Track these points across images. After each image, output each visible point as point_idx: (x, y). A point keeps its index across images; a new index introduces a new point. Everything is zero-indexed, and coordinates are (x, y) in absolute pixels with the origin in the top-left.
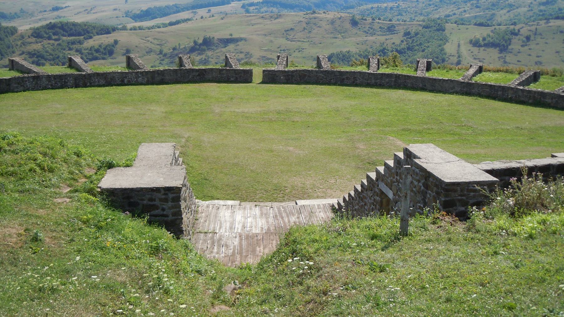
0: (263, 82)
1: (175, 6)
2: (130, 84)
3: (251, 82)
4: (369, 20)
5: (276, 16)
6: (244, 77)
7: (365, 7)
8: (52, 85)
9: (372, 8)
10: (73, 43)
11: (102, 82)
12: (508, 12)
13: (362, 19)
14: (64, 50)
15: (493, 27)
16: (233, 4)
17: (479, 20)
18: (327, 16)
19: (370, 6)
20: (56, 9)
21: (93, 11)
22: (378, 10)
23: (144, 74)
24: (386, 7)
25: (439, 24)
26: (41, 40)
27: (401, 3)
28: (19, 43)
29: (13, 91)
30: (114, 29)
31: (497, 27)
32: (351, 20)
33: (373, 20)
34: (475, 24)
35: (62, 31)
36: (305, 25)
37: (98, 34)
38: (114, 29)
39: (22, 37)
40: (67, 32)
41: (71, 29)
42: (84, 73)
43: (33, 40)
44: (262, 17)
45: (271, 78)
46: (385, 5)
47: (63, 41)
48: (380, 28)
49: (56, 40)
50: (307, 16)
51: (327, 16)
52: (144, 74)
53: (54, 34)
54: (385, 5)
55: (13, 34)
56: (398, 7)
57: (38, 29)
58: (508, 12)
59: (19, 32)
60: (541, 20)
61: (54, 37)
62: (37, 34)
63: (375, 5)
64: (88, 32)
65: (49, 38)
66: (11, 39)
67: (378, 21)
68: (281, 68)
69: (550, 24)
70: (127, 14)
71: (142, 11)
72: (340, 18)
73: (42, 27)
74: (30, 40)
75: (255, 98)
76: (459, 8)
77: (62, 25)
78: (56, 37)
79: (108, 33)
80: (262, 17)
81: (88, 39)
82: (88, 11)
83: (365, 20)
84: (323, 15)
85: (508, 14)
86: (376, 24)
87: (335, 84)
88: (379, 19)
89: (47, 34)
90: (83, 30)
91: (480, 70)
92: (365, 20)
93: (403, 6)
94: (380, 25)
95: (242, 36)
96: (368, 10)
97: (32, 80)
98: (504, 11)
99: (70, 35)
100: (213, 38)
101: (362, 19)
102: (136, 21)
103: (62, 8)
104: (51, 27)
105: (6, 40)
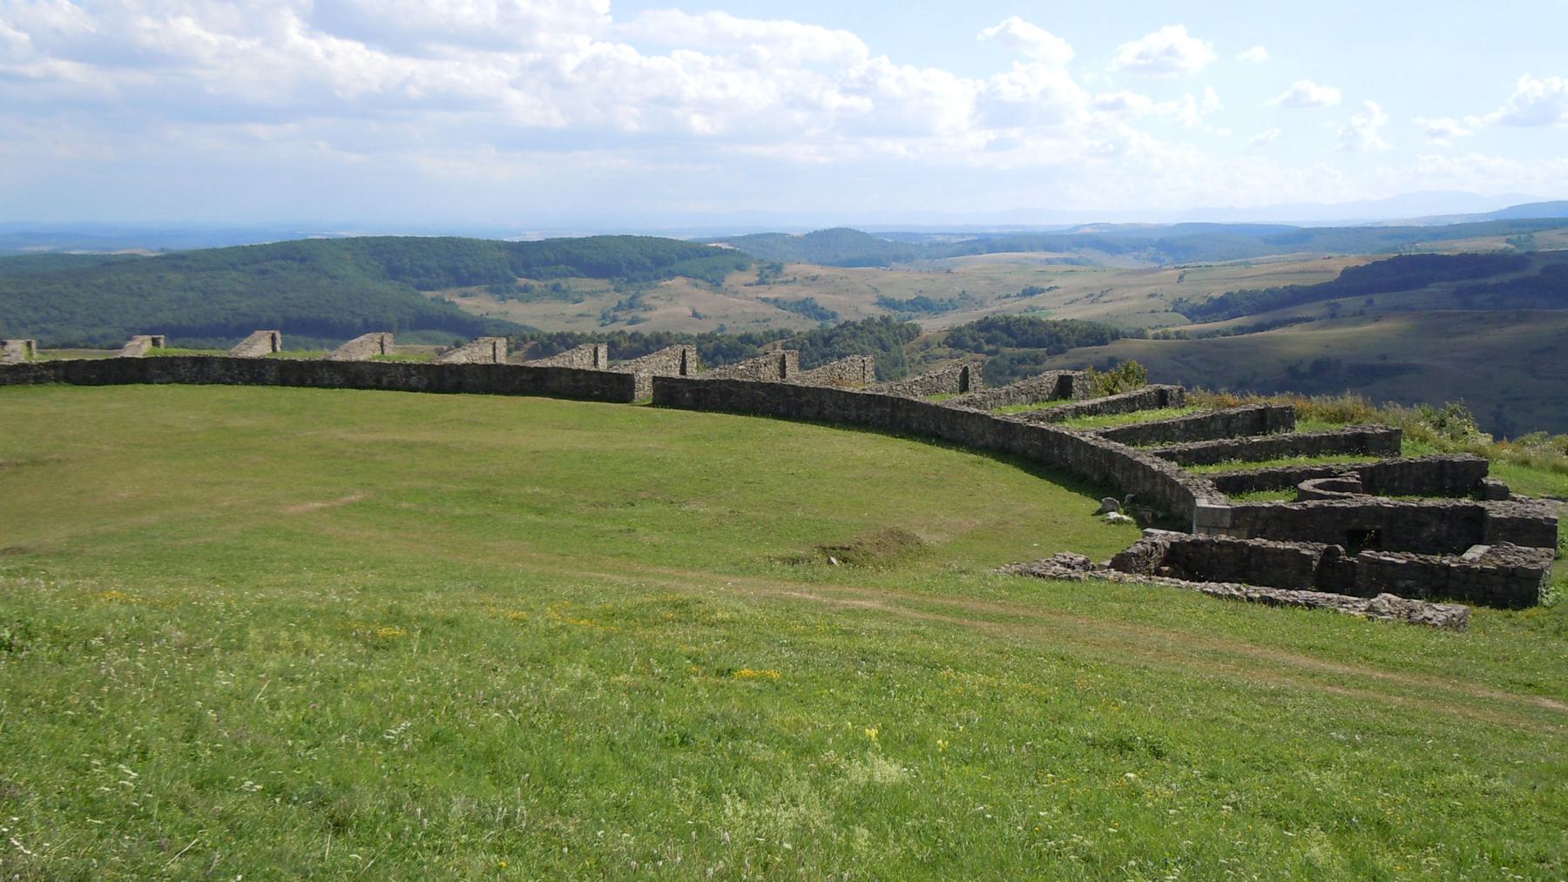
1: (1291, 289)
10: (1022, 361)
14: (1001, 373)
16: (1433, 288)
20: (1030, 292)
21: (1105, 298)
26: (959, 351)
28: (918, 357)
30: (1116, 336)
35: (1005, 336)
37: (1079, 345)
38: (1116, 336)
39: (927, 345)
40: (1015, 338)
41: (1026, 332)
43: (946, 351)
47: (1003, 356)
49: (988, 353)
53: (988, 342)
55: (910, 338)
57: (959, 330)
59: (924, 334)
61: (986, 348)
62: (955, 340)
64: (1059, 340)
65: (978, 350)
66: (905, 348)
70: (1177, 306)
71: (1211, 299)
73: (970, 326)
74: (939, 351)
77: (1008, 323)
78: (991, 347)
79: (1103, 342)
81: (1055, 353)
82: (1093, 299)
89: (974, 340)
90: (1050, 335)
95: (1416, 361)
99: (1019, 345)
100: (1338, 362)
102: (1194, 322)
103: (1043, 291)
104: (986, 326)
105: (894, 349)
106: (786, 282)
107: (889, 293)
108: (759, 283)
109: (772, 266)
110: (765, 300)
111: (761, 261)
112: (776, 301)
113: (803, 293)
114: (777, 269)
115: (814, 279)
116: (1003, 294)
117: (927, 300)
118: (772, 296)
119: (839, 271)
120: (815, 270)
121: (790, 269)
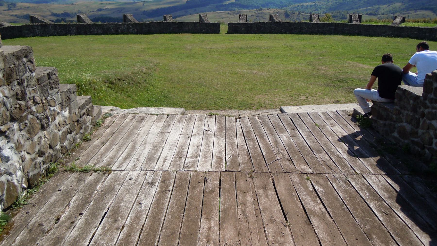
0: (228, 33)
2: (123, 33)
3: (219, 33)
4: (297, 13)
5: (237, 12)
6: (213, 28)
7: (293, 6)
8: (57, 33)
9: (298, 6)
11: (100, 31)
12: (389, 6)
13: (292, 13)
15: (379, 16)
17: (369, 12)
18: (269, 11)
19: (297, 5)
22: (302, 8)
23: (134, 25)
24: (307, 5)
25: (343, 15)
27: (317, 2)
29: (24, 36)
31: (382, 16)
32: (285, 14)
33: (299, 13)
34: (367, 14)
36: (255, 18)
42: (85, 24)
44: (228, 13)
45: (234, 29)
46: (307, 4)
48: (304, 18)
50: (257, 12)
51: (269, 11)
52: (134, 25)
54: (307, 4)
56: (315, 5)
58: (389, 6)
60: (411, 10)
63: (300, 4)
67: (302, 13)
68: (244, 22)
69: (417, 13)
72: (277, 13)
75: (222, 41)
76: (356, 5)
80: (228, 13)
83: (294, 13)
84: (266, 11)
85: (388, 8)
86: (301, 16)
87: (285, 33)
88: (303, 12)
91: (403, 20)
92: (294, 13)
93: (319, 4)
94: (304, 16)
96: (295, 7)
97: (40, 28)
98: (386, 6)
101: (292, 13)
106: (18, 9)
107: (55, 12)
108: (9, 9)
109: (12, 4)
110: (12, 15)
111: (8, 2)
112: (16, 15)
113: (25, 13)
114: (14, 5)
115: (28, 8)
116: (92, 11)
117: (67, 13)
118: (14, 14)
119: (36, 5)
120: (28, 5)
121: (19, 4)
